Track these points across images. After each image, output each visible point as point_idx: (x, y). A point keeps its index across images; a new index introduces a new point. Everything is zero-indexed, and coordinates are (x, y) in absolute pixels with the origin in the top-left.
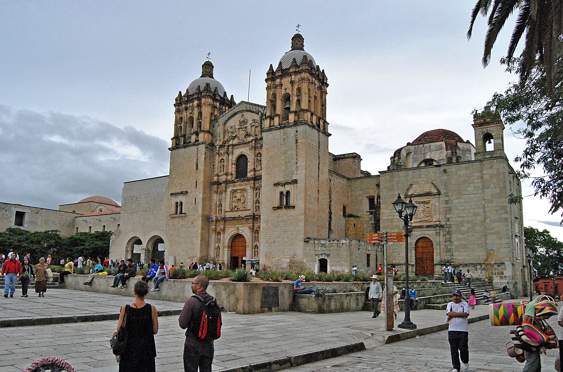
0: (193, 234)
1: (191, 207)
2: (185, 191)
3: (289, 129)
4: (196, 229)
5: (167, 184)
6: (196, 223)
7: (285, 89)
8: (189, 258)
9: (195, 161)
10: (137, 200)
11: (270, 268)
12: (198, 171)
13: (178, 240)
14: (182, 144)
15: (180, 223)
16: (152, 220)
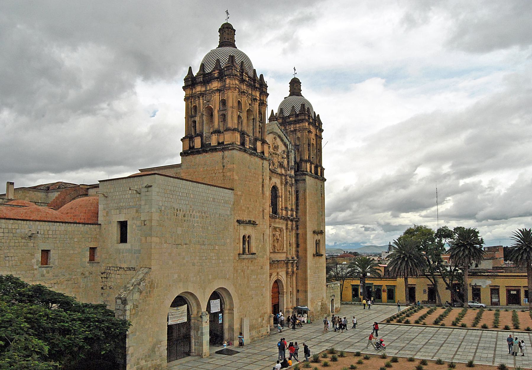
0: (263, 282)
1: (260, 246)
2: (253, 221)
3: (318, 181)
4: (265, 275)
5: (232, 204)
6: (265, 268)
7: (313, 139)
8: (260, 317)
9: (261, 180)
10: (186, 218)
11: (313, 312)
12: (264, 196)
13: (249, 293)
14: (248, 147)
15: (250, 267)
16: (213, 262)
